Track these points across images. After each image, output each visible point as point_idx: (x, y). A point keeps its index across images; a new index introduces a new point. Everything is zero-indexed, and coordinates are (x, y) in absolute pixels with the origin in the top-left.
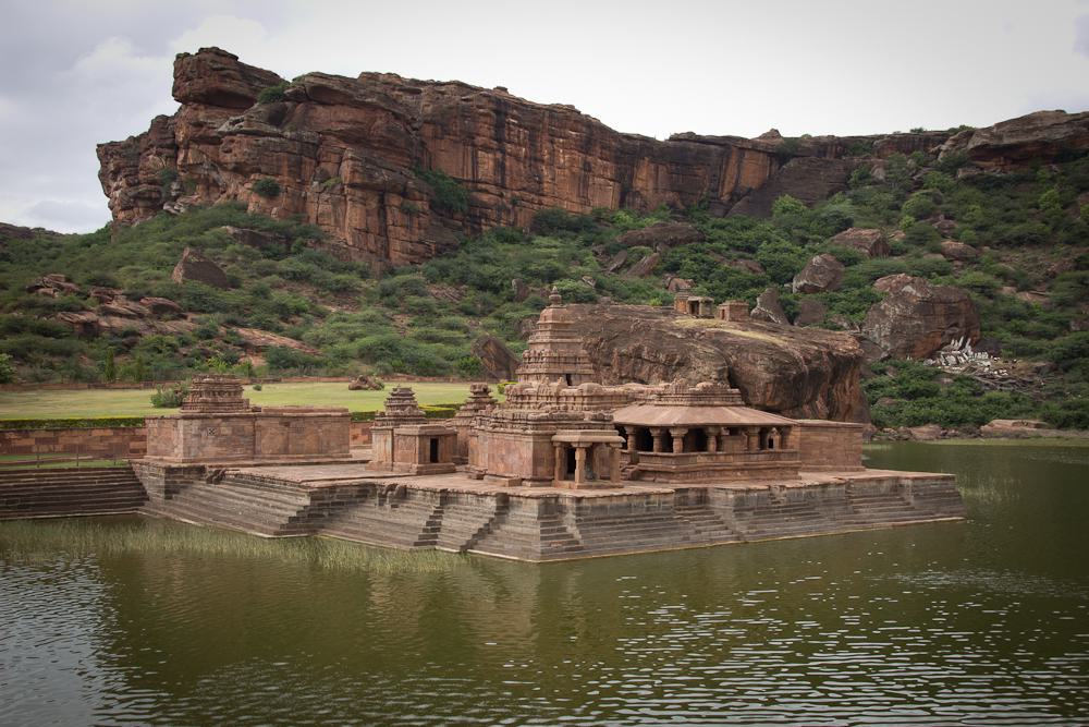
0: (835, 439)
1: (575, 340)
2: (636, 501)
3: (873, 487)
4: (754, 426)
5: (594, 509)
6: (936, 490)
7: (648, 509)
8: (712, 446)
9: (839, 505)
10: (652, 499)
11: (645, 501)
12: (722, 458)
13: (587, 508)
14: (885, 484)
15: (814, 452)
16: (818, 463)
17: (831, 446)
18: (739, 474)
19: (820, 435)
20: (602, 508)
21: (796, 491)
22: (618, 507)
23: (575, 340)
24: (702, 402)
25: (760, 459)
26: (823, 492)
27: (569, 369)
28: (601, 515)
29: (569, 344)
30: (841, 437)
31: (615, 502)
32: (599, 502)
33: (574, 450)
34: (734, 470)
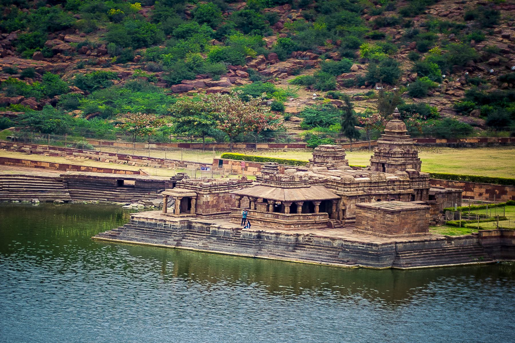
0: (375, 216)
1: (392, 143)
2: (159, 223)
3: (328, 242)
4: (270, 200)
5: (139, 222)
6: (363, 250)
7: (165, 227)
8: (253, 207)
9: (283, 246)
10: (167, 223)
11: (163, 223)
12: (252, 213)
13: (136, 222)
14: (337, 242)
15: (363, 222)
16: (366, 229)
17: (373, 220)
18: (259, 222)
19: (367, 212)
20: (143, 223)
21: (249, 233)
22: (151, 224)
23: (392, 143)
24: (266, 184)
25: (269, 217)
26: (277, 237)
27: (383, 160)
28: (143, 226)
29: (390, 145)
30: (379, 216)
31: (149, 221)
32: (142, 220)
33: (191, 199)
34: (258, 220)
